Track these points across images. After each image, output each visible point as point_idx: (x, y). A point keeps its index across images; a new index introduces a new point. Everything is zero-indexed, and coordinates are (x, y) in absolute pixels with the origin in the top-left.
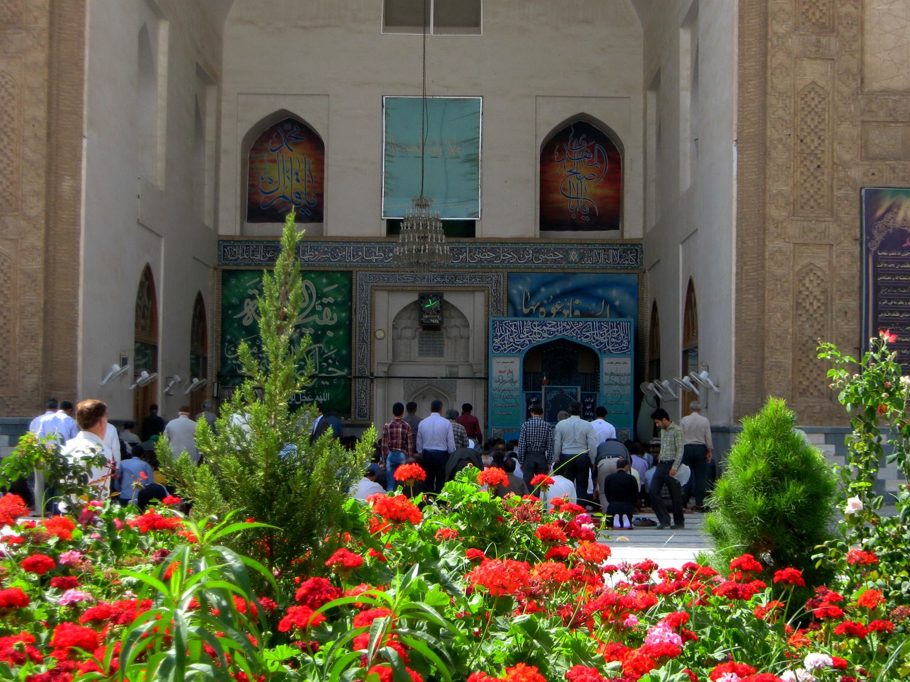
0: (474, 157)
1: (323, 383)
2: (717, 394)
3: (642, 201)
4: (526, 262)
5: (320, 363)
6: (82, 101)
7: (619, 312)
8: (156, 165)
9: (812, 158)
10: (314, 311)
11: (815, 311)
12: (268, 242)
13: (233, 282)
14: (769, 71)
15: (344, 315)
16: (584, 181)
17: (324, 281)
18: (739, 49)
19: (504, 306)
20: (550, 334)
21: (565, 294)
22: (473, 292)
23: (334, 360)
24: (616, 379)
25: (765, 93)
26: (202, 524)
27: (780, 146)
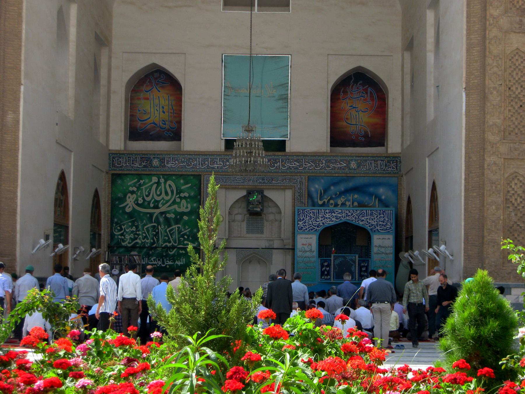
0: (284, 96)
1: (181, 252)
2: (452, 261)
3: (400, 127)
4: (321, 169)
5: (179, 238)
6: (20, 60)
7: (384, 204)
8: (68, 102)
9: (516, 100)
10: (174, 202)
11: (518, 205)
12: (143, 154)
13: (119, 182)
14: (487, 42)
15: (195, 205)
17: (182, 181)
18: (467, 26)
19: (305, 199)
20: (337, 219)
22: (284, 189)
23: (188, 236)
24: (383, 250)
25: (485, 57)
26: (195, 336)
27: (495, 92)
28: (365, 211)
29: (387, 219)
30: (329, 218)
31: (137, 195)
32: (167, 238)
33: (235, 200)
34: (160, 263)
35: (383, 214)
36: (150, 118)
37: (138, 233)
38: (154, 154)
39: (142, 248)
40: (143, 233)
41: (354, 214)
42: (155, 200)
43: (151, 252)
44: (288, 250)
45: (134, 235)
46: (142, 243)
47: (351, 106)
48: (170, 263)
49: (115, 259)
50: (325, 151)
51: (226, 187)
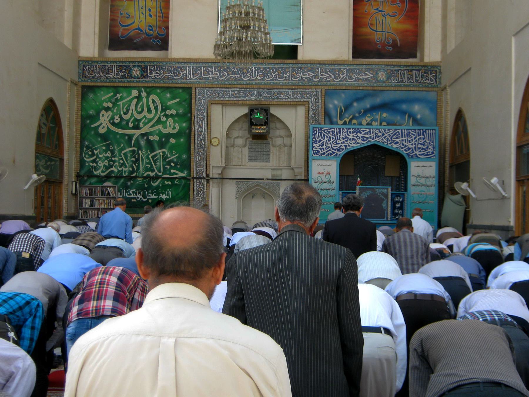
1: (166, 183)
3: (440, 30)
4: (341, 81)
5: (164, 166)
10: (159, 121)
12: (122, 62)
13: (91, 96)
15: (184, 125)
16: (389, 19)
17: (168, 95)
19: (321, 118)
20: (364, 140)
21: (374, 108)
23: (176, 164)
24: (422, 181)
28: (400, 131)
29: (428, 142)
30: (353, 139)
31: (112, 112)
32: (149, 166)
33: (234, 119)
34: (140, 197)
35: (423, 135)
36: (134, 22)
37: (113, 159)
38: (134, 62)
40: (120, 159)
41: (386, 135)
42: (135, 118)
43: (129, 184)
45: (109, 161)
46: (119, 171)
47: (377, 9)
48: (153, 197)
49: (85, 191)
50: (347, 59)
51: (223, 102)
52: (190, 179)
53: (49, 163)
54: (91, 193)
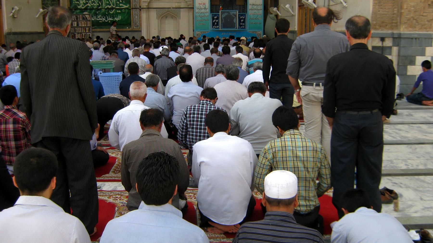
1: (118, 11)
5: (116, 2)
24: (255, 7)
32: (108, 2)
34: (104, 19)
39: (91, 9)
43: (97, 12)
44: (190, 9)
46: (91, 6)
48: (111, 19)
52: (130, 9)
53: (53, 3)
54: (77, 19)
